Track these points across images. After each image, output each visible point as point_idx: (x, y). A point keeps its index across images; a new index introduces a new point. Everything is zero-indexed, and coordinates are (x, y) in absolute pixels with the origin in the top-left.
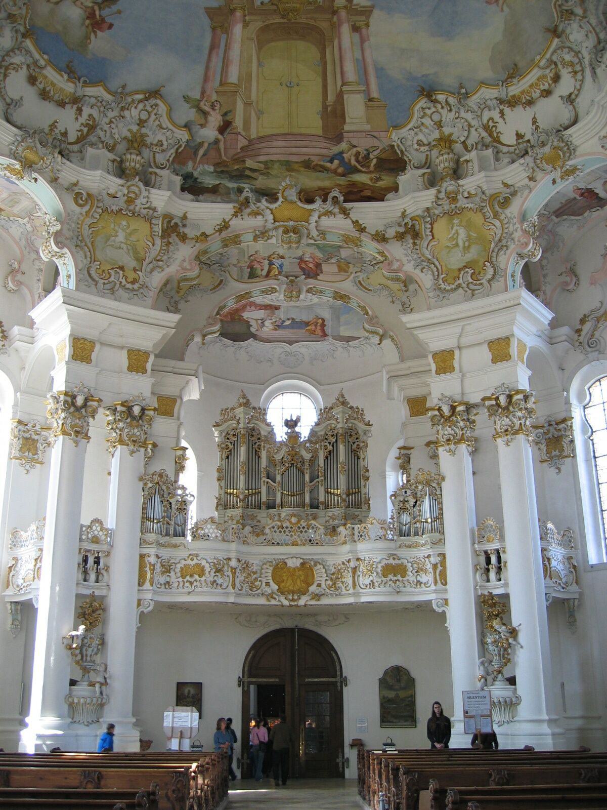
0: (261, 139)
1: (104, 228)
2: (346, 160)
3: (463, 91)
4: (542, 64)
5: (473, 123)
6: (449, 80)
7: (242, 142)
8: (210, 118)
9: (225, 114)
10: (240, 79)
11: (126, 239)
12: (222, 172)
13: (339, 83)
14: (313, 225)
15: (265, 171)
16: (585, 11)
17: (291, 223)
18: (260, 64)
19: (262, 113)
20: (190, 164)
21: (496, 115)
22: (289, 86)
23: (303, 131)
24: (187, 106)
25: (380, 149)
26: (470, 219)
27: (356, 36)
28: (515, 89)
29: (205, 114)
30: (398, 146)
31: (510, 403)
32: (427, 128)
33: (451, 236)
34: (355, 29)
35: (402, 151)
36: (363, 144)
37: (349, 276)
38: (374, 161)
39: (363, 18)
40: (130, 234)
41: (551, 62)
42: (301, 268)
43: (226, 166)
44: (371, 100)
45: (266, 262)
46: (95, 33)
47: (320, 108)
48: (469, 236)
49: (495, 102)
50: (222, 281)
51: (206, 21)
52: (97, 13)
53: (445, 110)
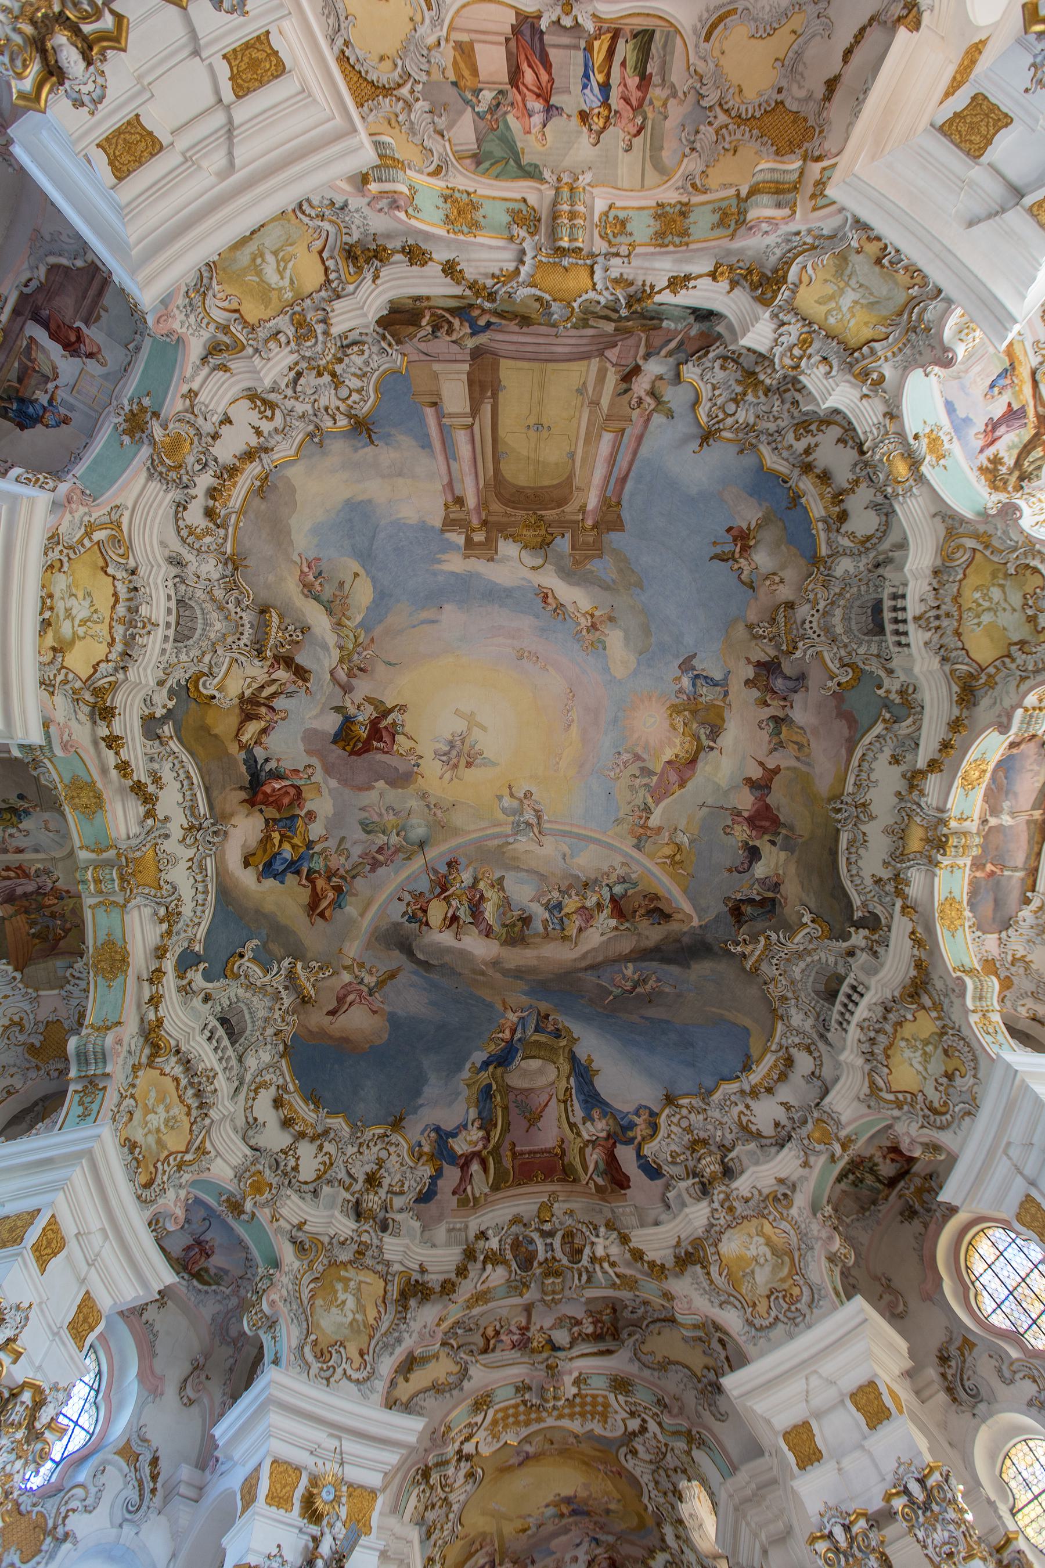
0: (585, 357)
1: (866, 324)
2: (467, 325)
3: (316, 440)
4: (234, 517)
5: (290, 404)
6: (338, 447)
7: (612, 354)
8: (647, 386)
9: (626, 391)
10: (599, 436)
11: (842, 291)
12: (652, 319)
13: (476, 427)
14: (528, 259)
15: (589, 316)
16: (213, 600)
17: (565, 262)
18: (572, 456)
19: (578, 391)
20: (693, 332)
21: (266, 427)
22: (539, 426)
23: (525, 364)
24: (673, 405)
25: (416, 340)
26: (266, 308)
27: (458, 493)
28: (253, 469)
29: (652, 393)
30: (390, 345)
31: (39, 45)
32: (354, 375)
33: (290, 265)
34: (460, 501)
35: (384, 338)
36: (442, 344)
37: (451, 28)
38: (424, 322)
39: (452, 516)
40: (832, 298)
41: (224, 526)
42: (547, 65)
43: (643, 325)
44: (434, 404)
45: (615, 101)
46: (749, 529)
47: (501, 395)
48: (259, 273)
49: (272, 442)
50: (707, 39)
51: (625, 515)
52: (738, 550)
53: (333, 406)
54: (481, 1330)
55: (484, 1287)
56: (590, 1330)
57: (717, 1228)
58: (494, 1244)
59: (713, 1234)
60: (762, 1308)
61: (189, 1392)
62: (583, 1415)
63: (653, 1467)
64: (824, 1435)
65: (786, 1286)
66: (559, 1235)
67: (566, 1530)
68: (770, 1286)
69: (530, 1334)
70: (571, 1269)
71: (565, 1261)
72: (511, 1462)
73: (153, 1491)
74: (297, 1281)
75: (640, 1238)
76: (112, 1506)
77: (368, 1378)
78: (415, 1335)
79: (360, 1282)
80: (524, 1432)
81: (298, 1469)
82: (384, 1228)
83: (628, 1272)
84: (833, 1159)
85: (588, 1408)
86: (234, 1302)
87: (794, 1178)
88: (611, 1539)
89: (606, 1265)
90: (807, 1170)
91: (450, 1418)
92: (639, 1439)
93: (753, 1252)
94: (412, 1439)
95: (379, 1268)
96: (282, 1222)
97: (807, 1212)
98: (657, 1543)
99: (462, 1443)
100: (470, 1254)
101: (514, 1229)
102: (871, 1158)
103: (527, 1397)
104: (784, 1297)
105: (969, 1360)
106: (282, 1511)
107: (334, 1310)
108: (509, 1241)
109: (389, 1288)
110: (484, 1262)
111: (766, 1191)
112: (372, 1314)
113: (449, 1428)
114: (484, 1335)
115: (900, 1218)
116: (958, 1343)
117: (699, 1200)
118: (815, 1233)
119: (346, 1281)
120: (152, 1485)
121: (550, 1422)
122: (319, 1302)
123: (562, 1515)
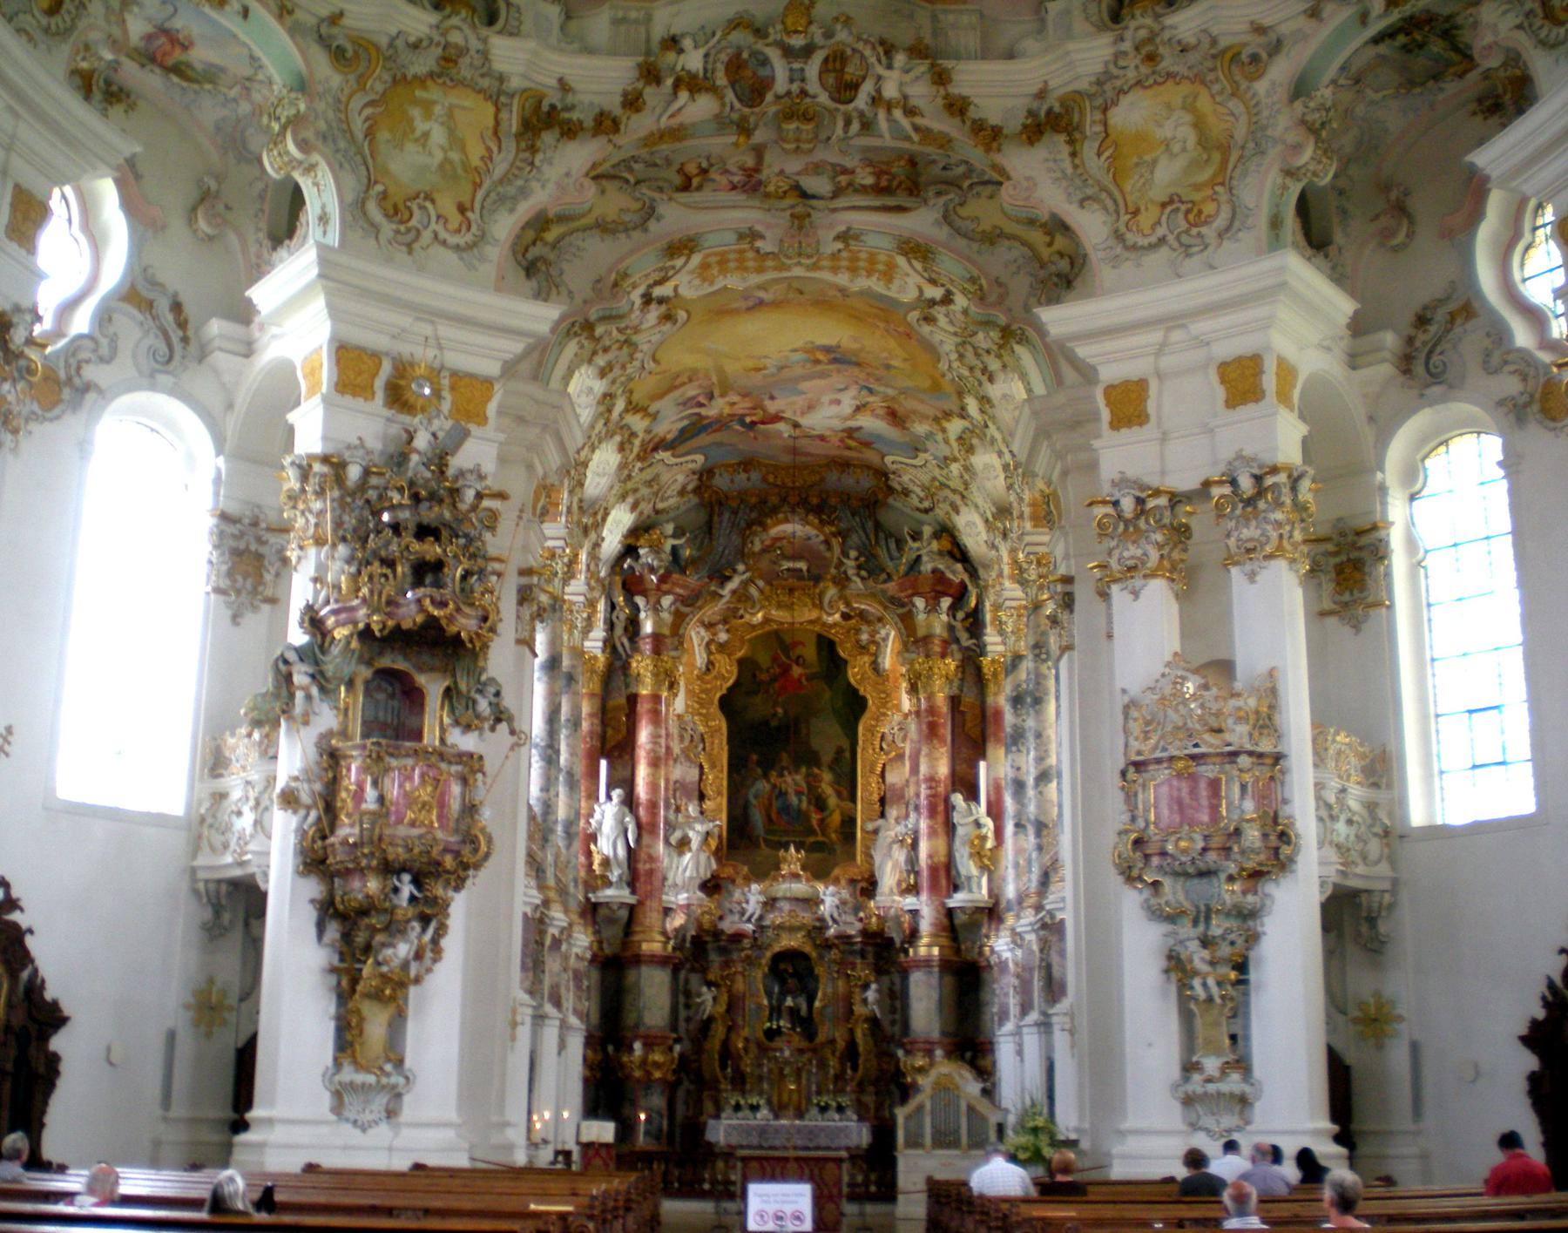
54: (676, 166)
55: (674, 122)
56: (869, 181)
57: (1118, 83)
58: (693, 61)
59: (1106, 93)
60: (1145, 220)
61: (202, 225)
62: (853, 270)
63: (959, 340)
64: (1161, 401)
65: (1197, 197)
66: (818, 59)
67: (823, 375)
68: (1172, 190)
69: (763, 176)
70: (832, 113)
71: (823, 98)
72: (735, 305)
73: (185, 340)
74: (341, 106)
75: (972, 78)
76: (134, 356)
77: (475, 244)
78: (551, 186)
79: (451, 107)
80: (755, 279)
81: (376, 356)
82: (491, 19)
83: (936, 126)
84: (1364, 18)
85: (861, 264)
86: (245, 108)
87: (1285, 29)
88: (890, 392)
89: (898, 114)
90: (1313, 23)
91: (624, 265)
92: (943, 309)
93: (1167, 131)
94: (544, 328)
95: (485, 83)
96: (300, 15)
97: (1282, 94)
98: (956, 409)
99: (650, 286)
100: (651, 74)
101: (740, 37)
102: (1449, 18)
103: (759, 244)
104: (1188, 212)
105: (1458, 330)
106: (361, 400)
107: (410, 147)
108: (724, 57)
109: (504, 115)
110: (676, 86)
111: (1224, 42)
112: (476, 153)
113: (625, 275)
114: (680, 171)
115: (1473, 106)
116: (1452, 306)
117: (1101, 28)
118: (1280, 129)
119: (427, 107)
120: (180, 333)
121: (798, 272)
122: (383, 135)
123: (817, 362)
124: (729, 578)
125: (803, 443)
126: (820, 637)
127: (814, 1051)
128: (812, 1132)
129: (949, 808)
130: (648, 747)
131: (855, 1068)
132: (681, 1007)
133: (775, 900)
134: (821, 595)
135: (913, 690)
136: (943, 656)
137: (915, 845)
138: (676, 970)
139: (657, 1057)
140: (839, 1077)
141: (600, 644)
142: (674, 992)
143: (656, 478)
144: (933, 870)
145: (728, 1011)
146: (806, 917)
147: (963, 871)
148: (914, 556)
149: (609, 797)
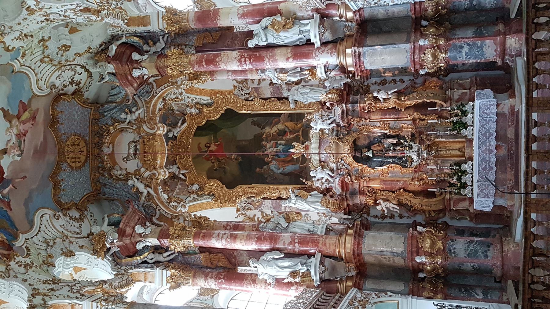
124: (137, 188)
125: (27, 146)
126: (195, 135)
127: (421, 133)
128: (484, 133)
129: (257, 48)
130: (224, 242)
131: (434, 104)
132: (392, 221)
133: (320, 162)
134: (148, 134)
135: (195, 76)
136: (166, 56)
137: (283, 71)
138: (367, 226)
139: (428, 244)
140: (440, 117)
141: (164, 271)
142: (380, 227)
143: (46, 242)
144: (296, 56)
145: (394, 192)
146: (331, 139)
147: (296, 37)
148: (112, 77)
149: (256, 267)
